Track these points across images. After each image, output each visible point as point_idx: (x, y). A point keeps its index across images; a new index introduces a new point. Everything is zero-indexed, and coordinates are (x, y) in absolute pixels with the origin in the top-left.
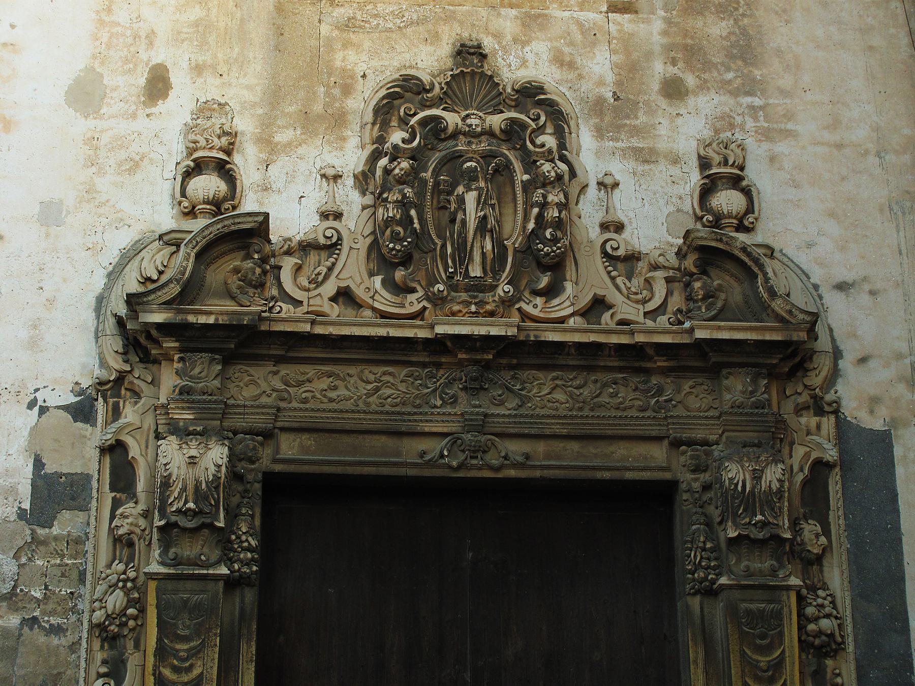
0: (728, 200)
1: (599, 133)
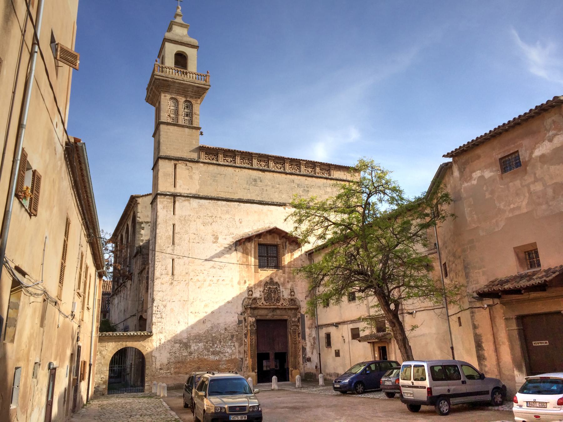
0: (293, 293)
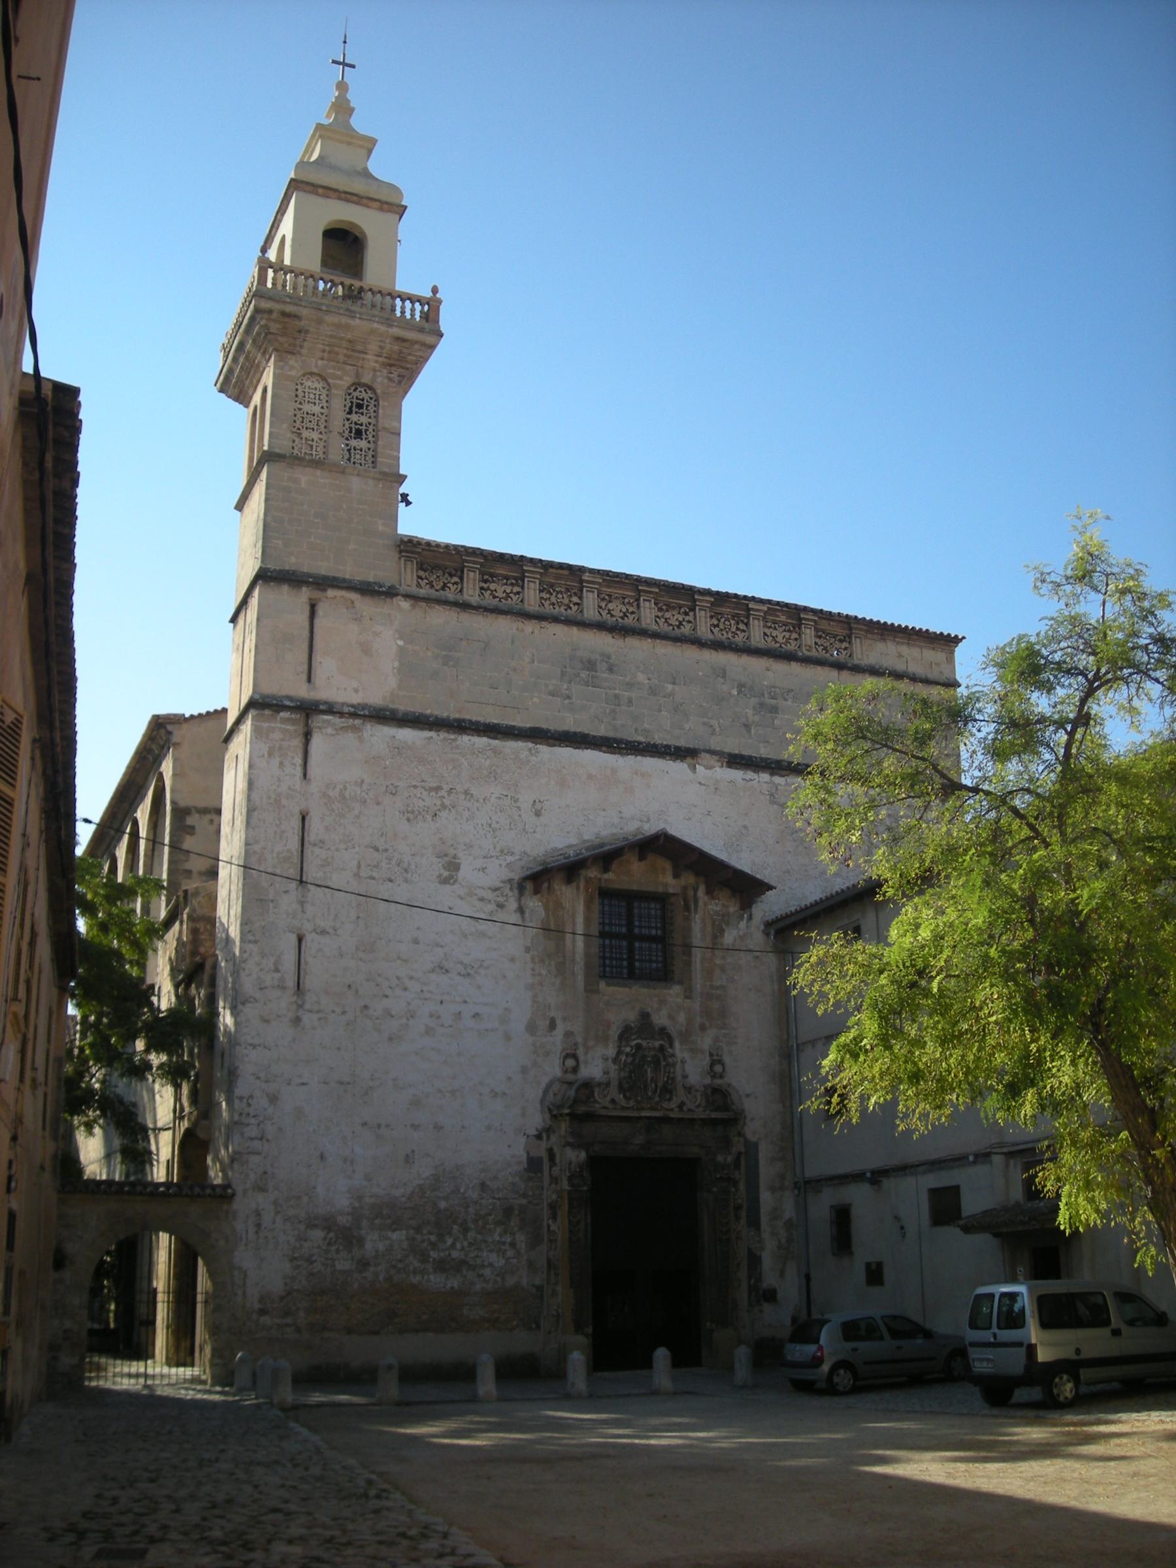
1: (681, 1043)
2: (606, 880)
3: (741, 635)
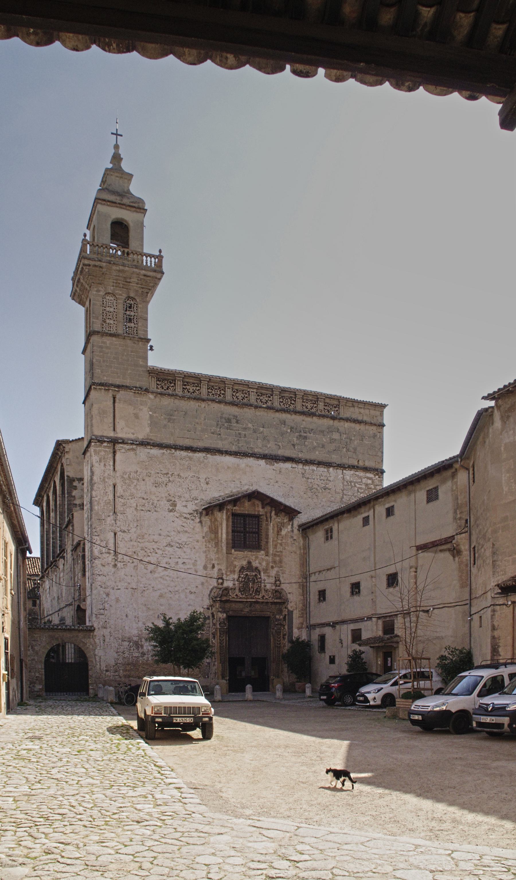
1: (264, 573)
2: (235, 510)
3: (292, 406)
